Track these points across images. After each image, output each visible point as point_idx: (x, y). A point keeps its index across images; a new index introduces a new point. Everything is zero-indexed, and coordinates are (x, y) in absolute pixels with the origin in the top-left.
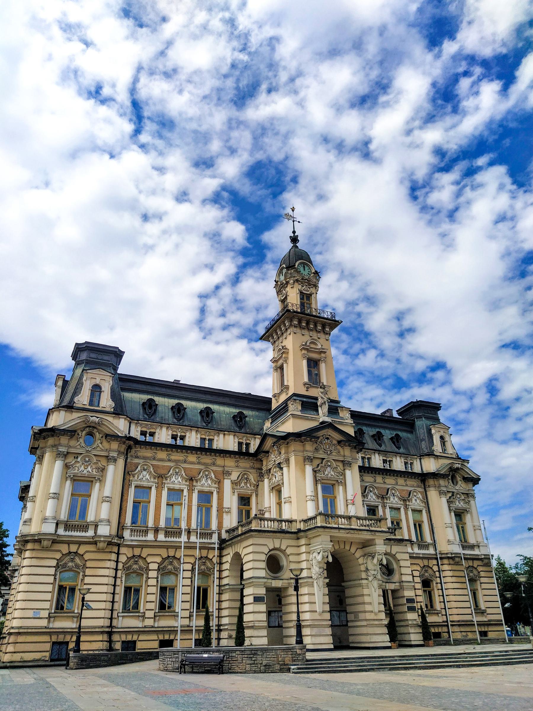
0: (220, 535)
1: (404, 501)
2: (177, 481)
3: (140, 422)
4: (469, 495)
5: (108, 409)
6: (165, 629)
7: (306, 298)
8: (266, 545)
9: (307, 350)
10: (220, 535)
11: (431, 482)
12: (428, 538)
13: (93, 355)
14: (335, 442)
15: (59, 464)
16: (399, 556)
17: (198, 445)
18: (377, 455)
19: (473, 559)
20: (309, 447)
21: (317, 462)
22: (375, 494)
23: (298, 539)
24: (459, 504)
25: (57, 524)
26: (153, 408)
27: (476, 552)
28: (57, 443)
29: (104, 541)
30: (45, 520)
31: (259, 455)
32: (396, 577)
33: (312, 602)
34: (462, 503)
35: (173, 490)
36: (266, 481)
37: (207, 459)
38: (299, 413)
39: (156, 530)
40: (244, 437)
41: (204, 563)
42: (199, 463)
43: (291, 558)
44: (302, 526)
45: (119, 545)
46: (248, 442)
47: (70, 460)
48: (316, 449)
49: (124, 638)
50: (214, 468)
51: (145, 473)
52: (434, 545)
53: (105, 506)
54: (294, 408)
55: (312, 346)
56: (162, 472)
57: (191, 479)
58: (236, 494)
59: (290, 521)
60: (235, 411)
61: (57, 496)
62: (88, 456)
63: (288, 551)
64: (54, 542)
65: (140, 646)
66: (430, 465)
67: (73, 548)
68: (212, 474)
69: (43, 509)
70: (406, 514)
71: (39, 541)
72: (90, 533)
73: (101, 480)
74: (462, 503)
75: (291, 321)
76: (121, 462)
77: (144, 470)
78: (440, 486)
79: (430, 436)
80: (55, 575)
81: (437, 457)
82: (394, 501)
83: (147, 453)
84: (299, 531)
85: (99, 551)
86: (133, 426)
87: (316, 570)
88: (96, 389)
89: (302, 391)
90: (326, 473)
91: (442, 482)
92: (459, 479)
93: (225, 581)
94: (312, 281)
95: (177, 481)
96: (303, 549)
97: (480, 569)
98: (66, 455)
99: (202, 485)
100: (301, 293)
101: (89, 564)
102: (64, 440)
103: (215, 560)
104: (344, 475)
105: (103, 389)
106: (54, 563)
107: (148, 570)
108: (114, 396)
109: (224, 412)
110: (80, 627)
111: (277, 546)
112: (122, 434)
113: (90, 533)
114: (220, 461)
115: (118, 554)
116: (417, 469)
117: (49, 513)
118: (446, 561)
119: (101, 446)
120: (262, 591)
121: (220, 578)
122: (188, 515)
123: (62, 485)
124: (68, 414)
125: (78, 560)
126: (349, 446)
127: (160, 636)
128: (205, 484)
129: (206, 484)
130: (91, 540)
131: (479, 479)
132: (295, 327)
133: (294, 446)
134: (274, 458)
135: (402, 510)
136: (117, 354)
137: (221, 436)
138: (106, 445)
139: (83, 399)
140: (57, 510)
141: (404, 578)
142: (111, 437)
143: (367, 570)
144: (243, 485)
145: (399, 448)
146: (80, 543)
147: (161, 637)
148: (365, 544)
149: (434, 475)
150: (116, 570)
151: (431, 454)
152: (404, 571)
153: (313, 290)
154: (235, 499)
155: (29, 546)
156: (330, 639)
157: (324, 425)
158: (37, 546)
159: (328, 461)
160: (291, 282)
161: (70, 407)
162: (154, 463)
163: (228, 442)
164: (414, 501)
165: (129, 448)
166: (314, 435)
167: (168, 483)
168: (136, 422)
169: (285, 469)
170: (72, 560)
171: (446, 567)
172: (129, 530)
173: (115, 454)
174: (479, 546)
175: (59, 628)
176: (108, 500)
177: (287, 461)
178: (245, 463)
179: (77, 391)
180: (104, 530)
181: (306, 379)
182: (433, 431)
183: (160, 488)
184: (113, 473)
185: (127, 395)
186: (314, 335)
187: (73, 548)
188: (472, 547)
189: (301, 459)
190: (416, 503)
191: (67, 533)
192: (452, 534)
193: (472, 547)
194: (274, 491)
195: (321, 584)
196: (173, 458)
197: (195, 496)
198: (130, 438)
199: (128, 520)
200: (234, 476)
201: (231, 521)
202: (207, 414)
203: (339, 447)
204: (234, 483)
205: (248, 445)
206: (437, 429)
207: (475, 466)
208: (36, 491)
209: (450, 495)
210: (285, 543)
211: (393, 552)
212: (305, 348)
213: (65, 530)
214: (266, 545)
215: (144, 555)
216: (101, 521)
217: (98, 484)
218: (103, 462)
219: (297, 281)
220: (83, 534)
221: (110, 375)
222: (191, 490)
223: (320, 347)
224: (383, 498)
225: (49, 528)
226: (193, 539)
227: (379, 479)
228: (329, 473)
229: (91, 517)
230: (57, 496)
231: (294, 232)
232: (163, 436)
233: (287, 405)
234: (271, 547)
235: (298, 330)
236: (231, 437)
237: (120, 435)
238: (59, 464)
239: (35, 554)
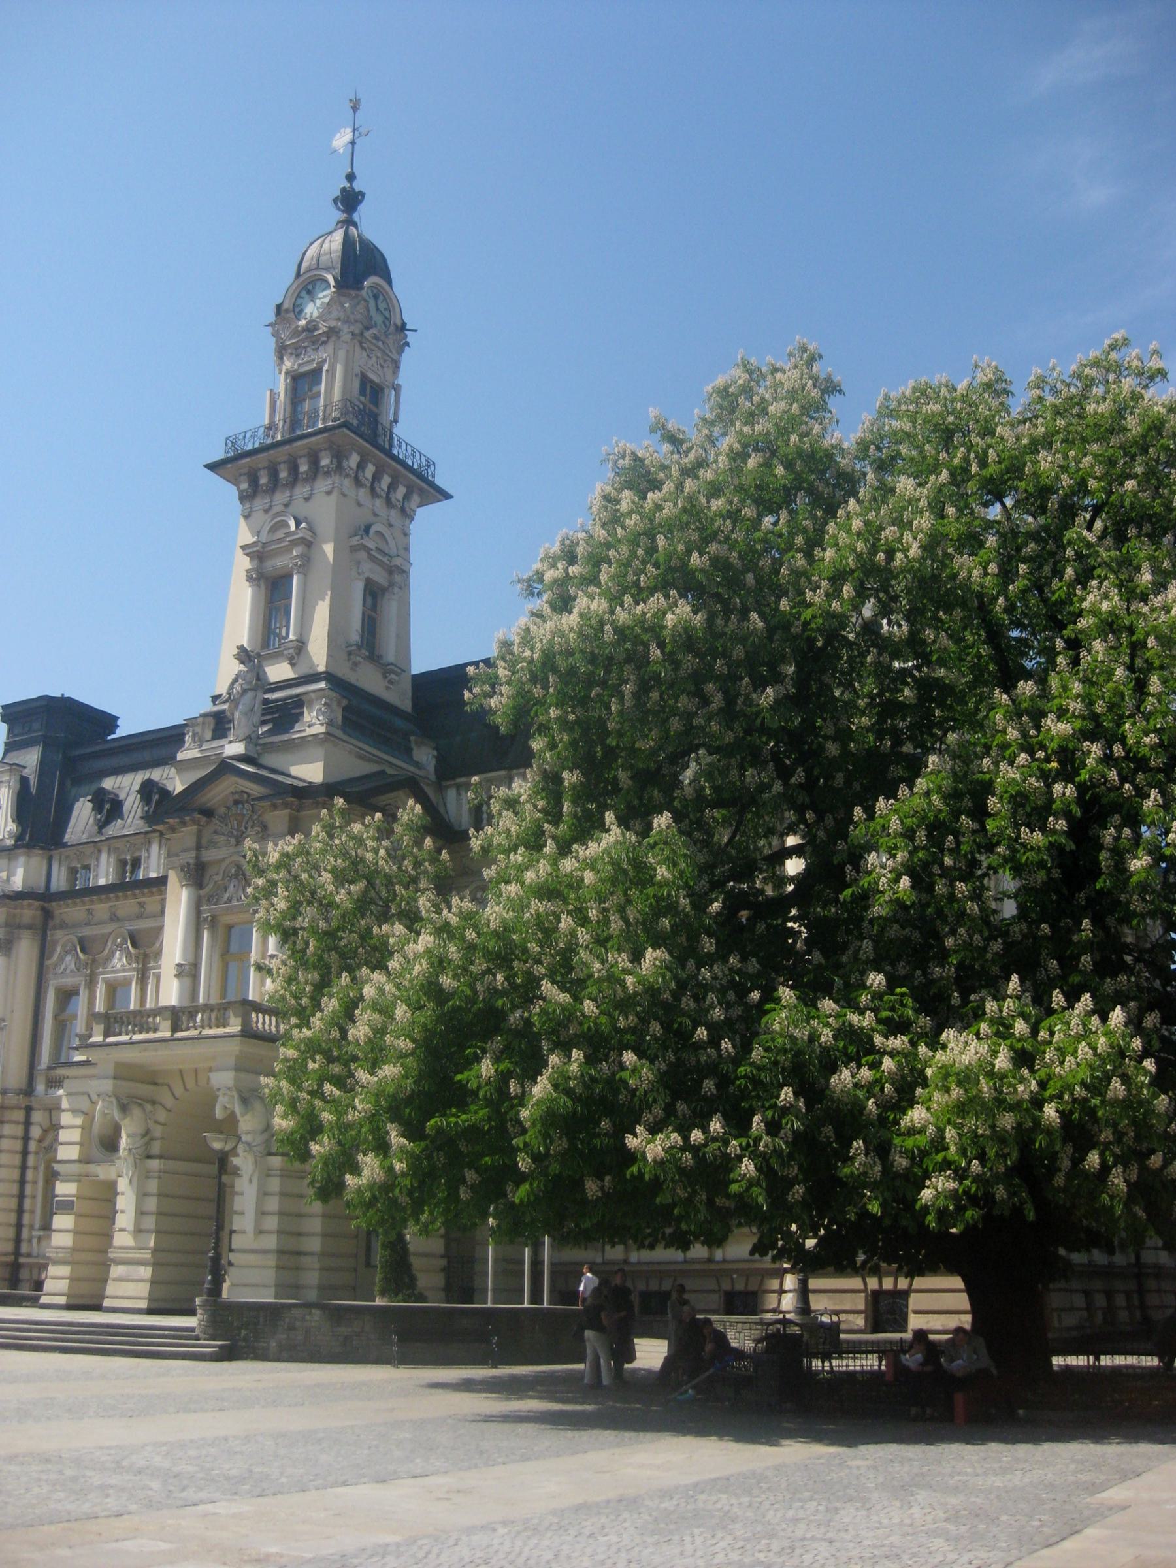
55: (280, 534)
83: (72, 912)
90: (227, 895)
115: (27, 1124)
150: (25, 1153)
167: (103, 973)
183: (91, 983)
186: (301, 490)
231: (351, 177)
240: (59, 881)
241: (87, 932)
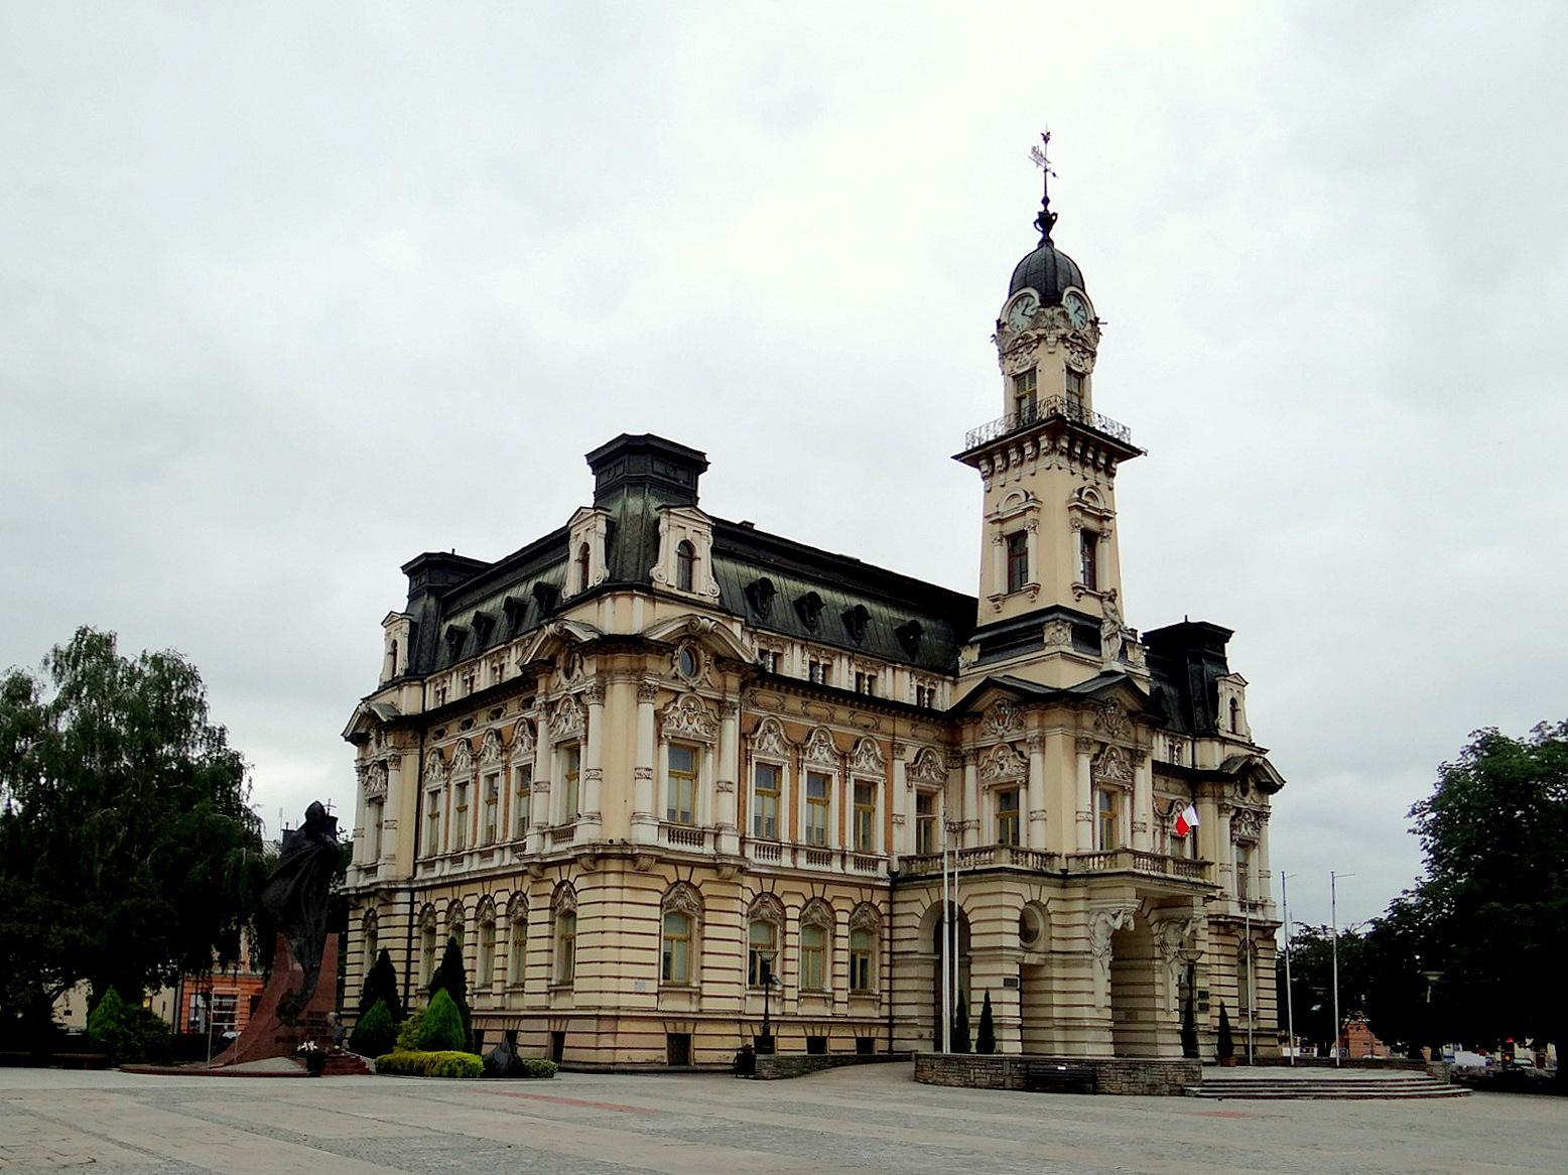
0: (889, 862)
2: (821, 759)
3: (759, 631)
4: (1262, 815)
5: (709, 600)
6: (855, 1020)
8: (1020, 895)
14: (1124, 714)
20: (1088, 720)
23: (1064, 887)
28: (635, 665)
29: (734, 866)
30: (636, 817)
34: (1249, 830)
36: (971, 770)
37: (865, 718)
39: (795, 850)
40: (928, 676)
42: (853, 725)
43: (1055, 919)
44: (1074, 868)
46: (932, 687)
51: (771, 737)
54: (1059, 637)
56: (799, 738)
57: (843, 757)
58: (914, 789)
59: (1049, 857)
61: (647, 774)
62: (692, 699)
63: (1051, 907)
64: (660, 861)
65: (833, 1045)
66: (1211, 756)
67: (684, 873)
68: (877, 749)
71: (633, 858)
72: (708, 848)
74: (1249, 830)
77: (770, 731)
78: (1222, 796)
81: (1224, 741)
85: (726, 881)
87: (1102, 942)
89: (1068, 602)
91: (1228, 790)
92: (1252, 784)
95: (821, 759)
99: (861, 770)
102: (651, 662)
103: (883, 909)
104: (1133, 777)
105: (698, 554)
106: (656, 898)
110: (766, 1015)
112: (750, 659)
113: (708, 848)
114: (886, 724)
116: (1187, 763)
122: (839, 825)
124: (649, 606)
125: (690, 893)
127: (808, 1031)
128: (865, 767)
129: (867, 768)
130: (712, 861)
131: (1281, 787)
133: (1060, 716)
137: (889, 671)
139: (666, 571)
142: (726, 662)
143: (1163, 944)
144: (924, 773)
146: (692, 865)
147: (810, 1034)
149: (1219, 777)
151: (1210, 732)
155: (614, 865)
158: (629, 867)
159: (1112, 749)
161: (647, 589)
163: (897, 685)
167: (808, 761)
168: (751, 629)
169: (1036, 759)
172: (753, 846)
174: (1263, 906)
175: (670, 1012)
177: (1042, 741)
178: (927, 733)
182: (1221, 688)
183: (797, 767)
187: (684, 873)
188: (1254, 907)
189: (1072, 741)
194: (992, 793)
195: (1107, 964)
196: (812, 710)
197: (850, 788)
200: (910, 754)
201: (906, 842)
204: (907, 768)
205: (931, 692)
207: (1278, 761)
210: (1046, 893)
214: (1020, 895)
217: (710, 756)
220: (696, 849)
221: (710, 522)
222: (844, 778)
225: (647, 835)
232: (795, 664)
233: (1040, 628)
236: (907, 675)
237: (747, 660)
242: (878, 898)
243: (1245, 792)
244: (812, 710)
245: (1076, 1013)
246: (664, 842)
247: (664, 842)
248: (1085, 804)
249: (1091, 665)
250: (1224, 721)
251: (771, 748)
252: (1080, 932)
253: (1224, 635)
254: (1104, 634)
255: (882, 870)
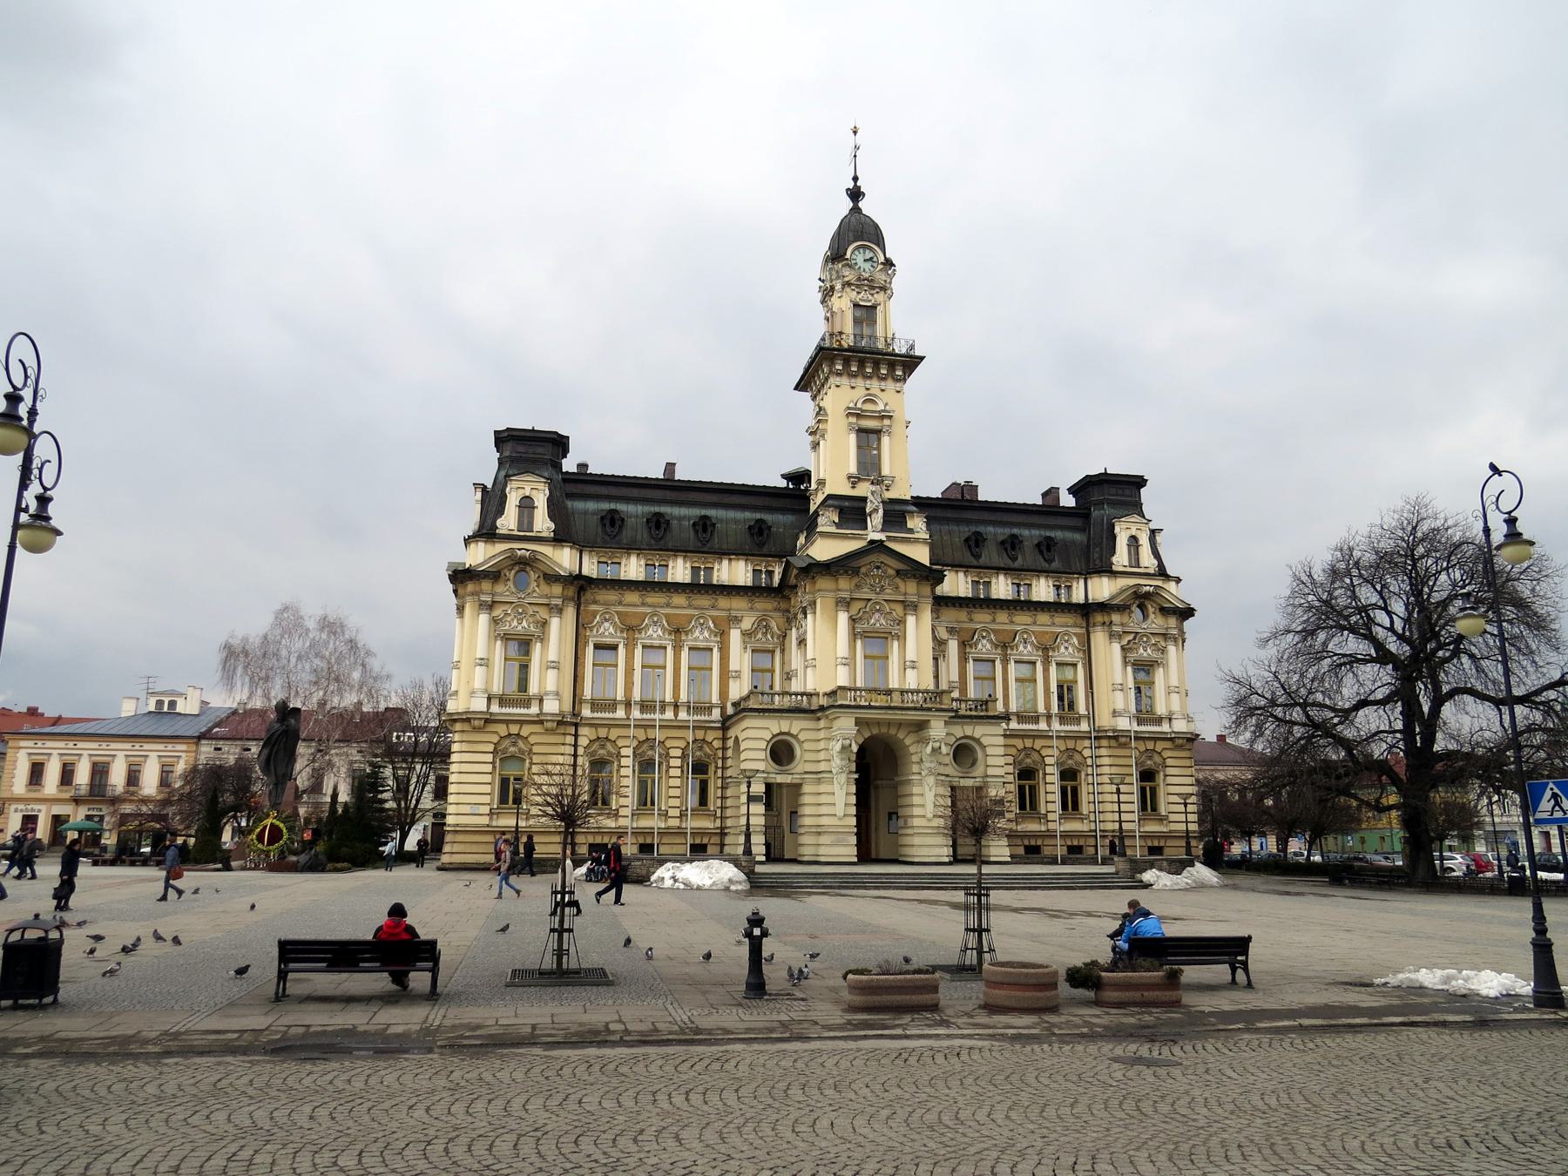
0: (723, 709)
1: (1045, 649)
2: (655, 634)
7: (866, 314)
9: (858, 416)
10: (723, 709)
11: (1099, 618)
12: (1081, 707)
13: (521, 449)
15: (484, 618)
16: (984, 741)
17: (688, 580)
18: (1001, 577)
19: (1155, 739)
20: (844, 583)
21: (856, 606)
22: (991, 641)
24: (1144, 653)
25: (489, 699)
26: (618, 523)
27: (1165, 728)
30: (473, 693)
31: (783, 591)
32: (979, 770)
33: (830, 805)
35: (652, 647)
37: (704, 601)
38: (833, 529)
39: (628, 705)
41: (701, 748)
42: (690, 606)
43: (806, 746)
44: (824, 701)
45: (576, 725)
47: (498, 612)
48: (858, 586)
49: (591, 840)
50: (714, 613)
52: (1091, 717)
53: (552, 674)
54: (828, 520)
55: (869, 407)
56: (634, 622)
57: (677, 631)
59: (810, 695)
60: (750, 516)
61: (485, 662)
63: (802, 737)
64: (487, 721)
66: (1102, 589)
67: (514, 729)
69: (470, 681)
70: (1046, 671)
71: (468, 720)
72: (534, 710)
73: (543, 639)
75: (832, 364)
76: (570, 612)
79: (1114, 537)
80: (493, 763)
82: (1025, 651)
83: (611, 596)
84: (822, 708)
85: (548, 731)
86: (586, 558)
87: (837, 762)
88: (527, 505)
89: (845, 489)
91: (1116, 618)
92: (1151, 610)
93: (729, 773)
94: (878, 282)
95: (655, 634)
96: (822, 734)
97: (1166, 754)
98: (490, 606)
99: (696, 639)
100: (856, 305)
101: (536, 749)
102: (486, 585)
103: (717, 744)
104: (902, 622)
106: (491, 748)
107: (619, 756)
108: (555, 510)
109: (731, 519)
111: (785, 729)
113: (534, 710)
114: (723, 602)
115: (576, 736)
116: (1078, 596)
117: (478, 683)
118: (1104, 743)
119: (538, 590)
120: (758, 788)
121: (724, 768)
123: (491, 649)
124: (489, 547)
125: (521, 743)
126: (914, 576)
128: (700, 636)
132: (839, 374)
133: (824, 583)
134: (801, 598)
135: (1039, 666)
136: (559, 444)
138: (545, 589)
139: (508, 521)
140: (488, 680)
141: (990, 771)
145: (1049, 561)
146: (522, 723)
148: (921, 726)
149: (1103, 607)
150: (575, 756)
151: (1107, 570)
152: (990, 761)
153: (880, 297)
154: (748, 656)
155: (458, 726)
156: (854, 851)
157: (876, 546)
158: (466, 727)
160: (838, 287)
162: (620, 609)
163: (736, 572)
164: (1062, 649)
165: (581, 590)
166: (855, 564)
170: (514, 744)
171: (1103, 752)
173: (559, 602)
176: (555, 665)
178: (764, 604)
179: (500, 511)
180: (551, 706)
181: (853, 469)
182: (1117, 529)
184: (560, 629)
185: (579, 505)
186: (875, 384)
187: (514, 729)
188: (1159, 721)
190: (1067, 652)
191: (504, 710)
192: (1125, 701)
193: (1159, 721)
198: (580, 576)
199: (587, 694)
200: (747, 624)
202: (704, 526)
203: (897, 580)
204: (745, 634)
205: (770, 574)
206: (1124, 526)
208: (461, 655)
209: (1131, 637)
210: (795, 726)
211: (977, 735)
212: (855, 413)
213: (501, 705)
215: (612, 737)
216: (547, 694)
218: (543, 613)
219: (849, 284)
222: (677, 649)
223: (881, 407)
224: (1005, 646)
225: (479, 705)
226: (683, 715)
227: (1002, 616)
228: (878, 621)
229: (533, 689)
230: (485, 662)
231: (855, 179)
232: (633, 568)
234: (776, 731)
235: (844, 381)
238: (484, 618)
239: (465, 737)
240: (590, 568)
241: (620, 609)
242: (710, 736)
243: (1145, 617)
244: (649, 600)
245: (824, 821)
246: (495, 708)
247: (495, 708)
248: (842, 649)
249: (859, 537)
250: (1121, 558)
251: (607, 631)
252: (822, 756)
253: (1139, 482)
254: (868, 510)
255: (716, 714)
